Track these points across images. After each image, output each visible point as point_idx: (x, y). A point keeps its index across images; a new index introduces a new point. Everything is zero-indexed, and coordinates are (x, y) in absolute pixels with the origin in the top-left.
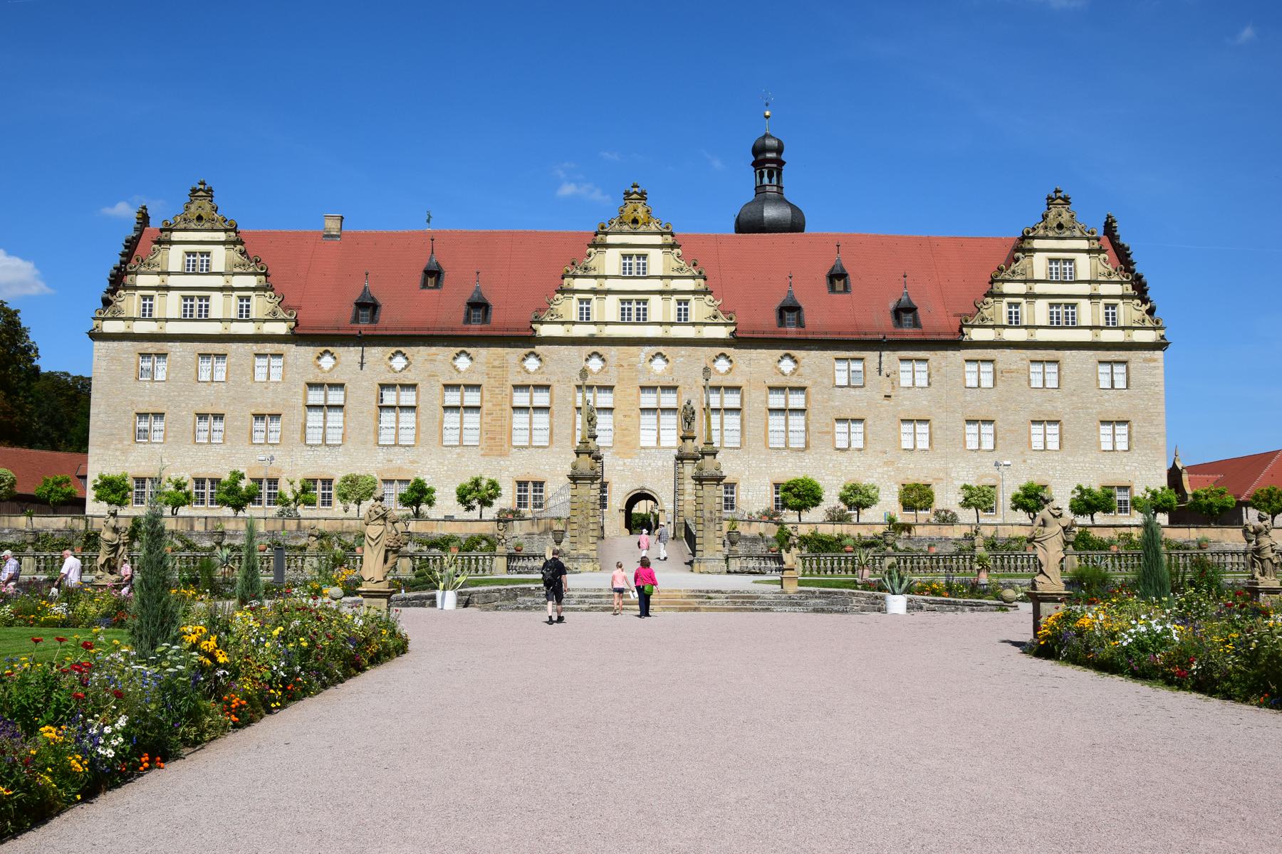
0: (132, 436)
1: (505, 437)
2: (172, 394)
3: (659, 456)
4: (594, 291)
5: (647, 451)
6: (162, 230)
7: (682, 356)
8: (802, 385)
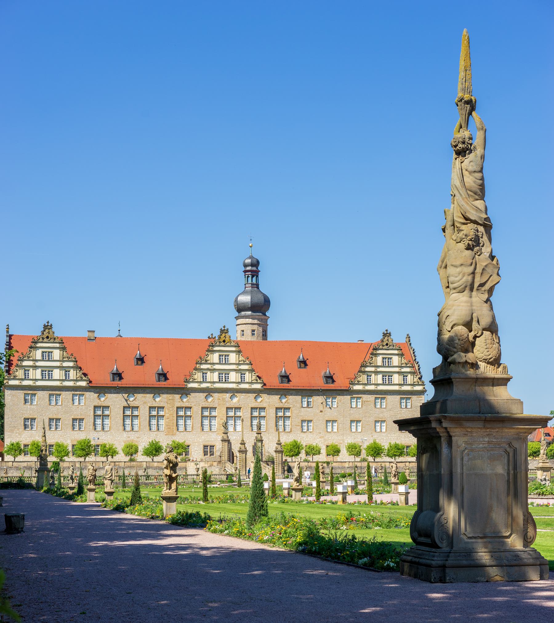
0: (23, 427)
1: (175, 428)
4: (208, 369)
6: (33, 342)
8: (289, 407)
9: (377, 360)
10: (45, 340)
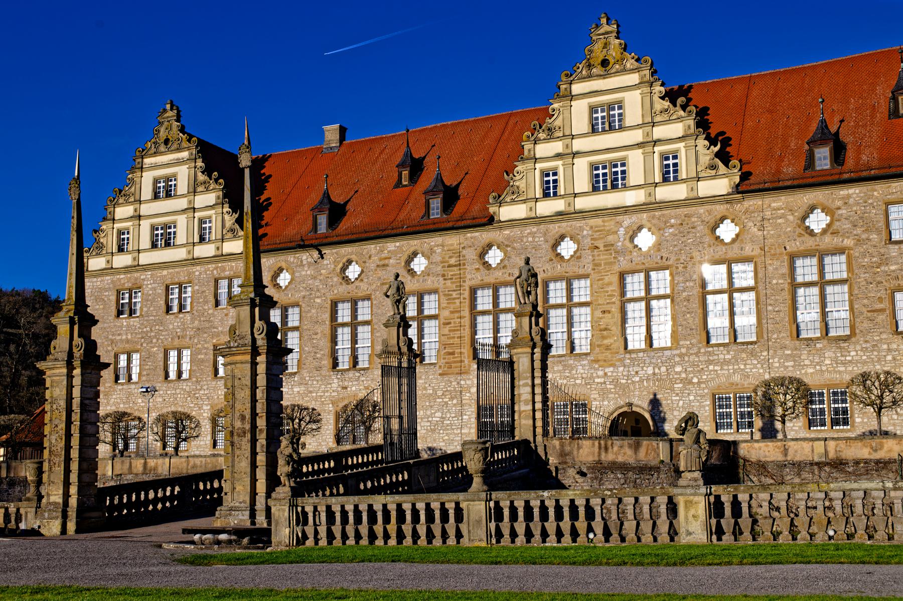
2: (145, 330)
3: (648, 361)
4: (558, 156)
5: (634, 356)
7: (672, 226)
10: (162, 148)
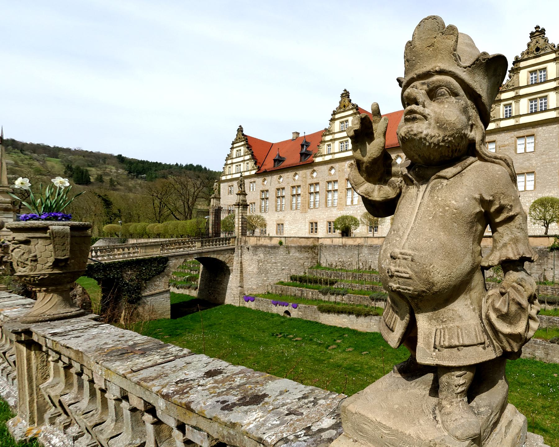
9: (518, 78)
